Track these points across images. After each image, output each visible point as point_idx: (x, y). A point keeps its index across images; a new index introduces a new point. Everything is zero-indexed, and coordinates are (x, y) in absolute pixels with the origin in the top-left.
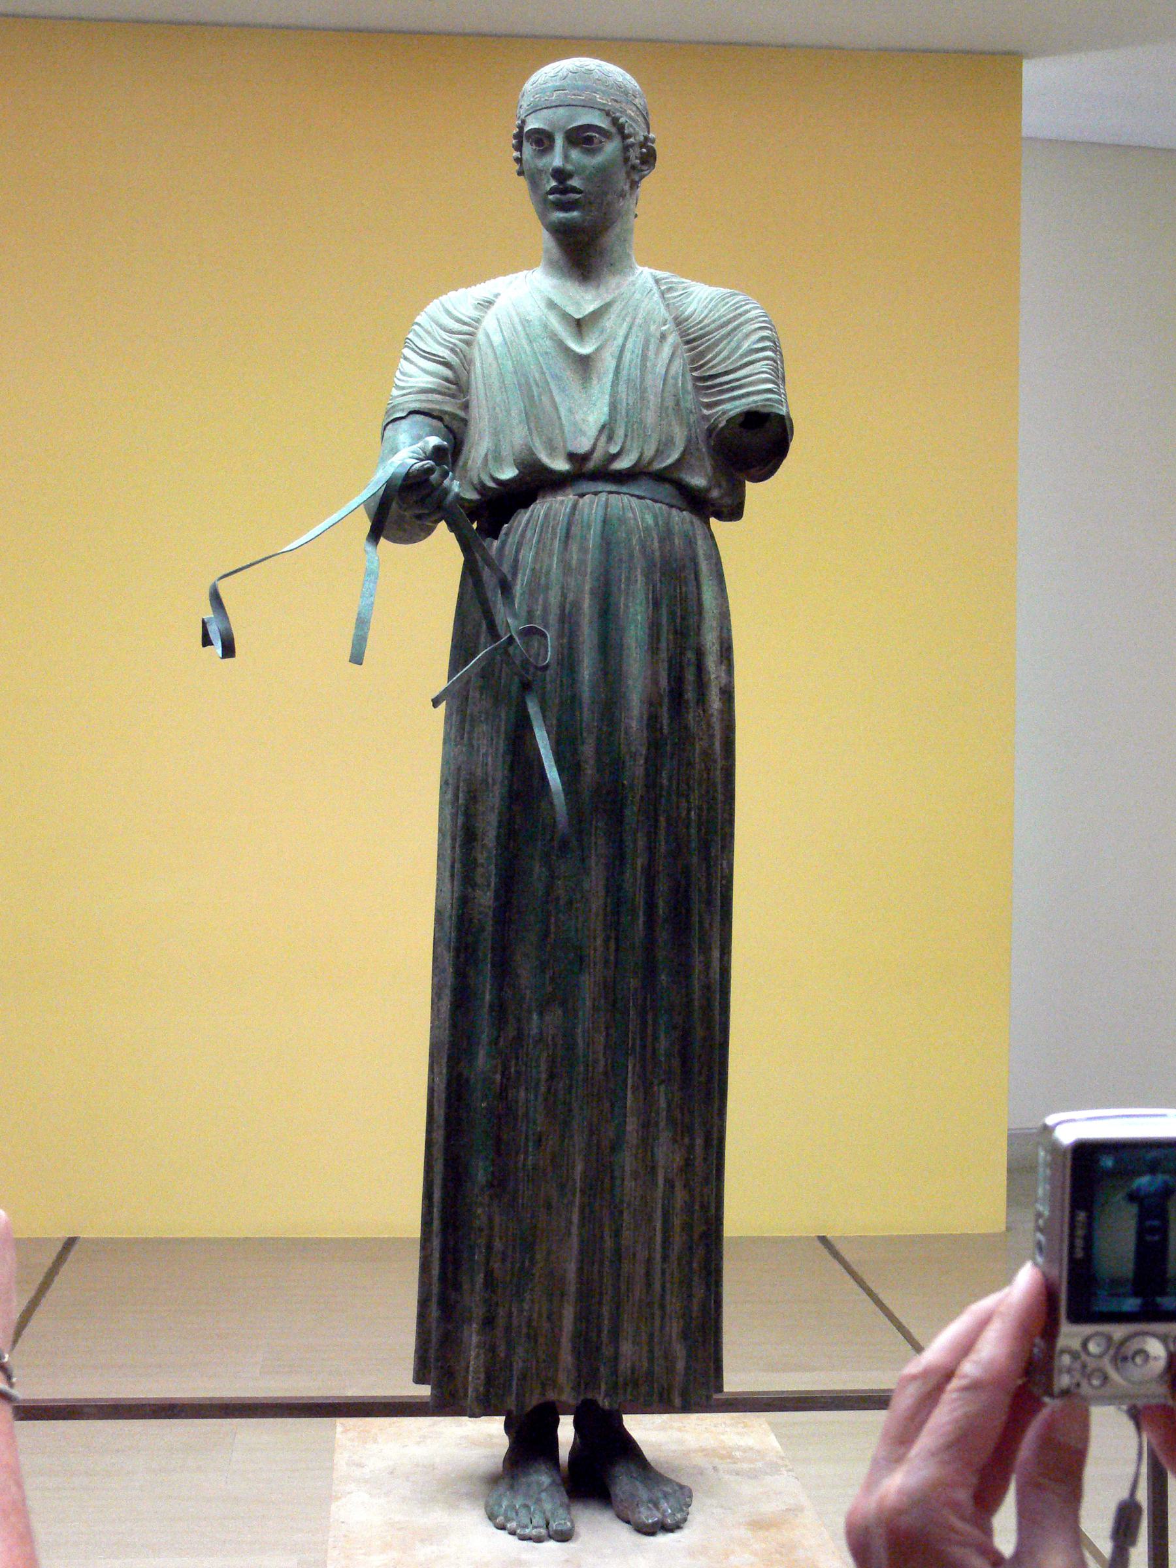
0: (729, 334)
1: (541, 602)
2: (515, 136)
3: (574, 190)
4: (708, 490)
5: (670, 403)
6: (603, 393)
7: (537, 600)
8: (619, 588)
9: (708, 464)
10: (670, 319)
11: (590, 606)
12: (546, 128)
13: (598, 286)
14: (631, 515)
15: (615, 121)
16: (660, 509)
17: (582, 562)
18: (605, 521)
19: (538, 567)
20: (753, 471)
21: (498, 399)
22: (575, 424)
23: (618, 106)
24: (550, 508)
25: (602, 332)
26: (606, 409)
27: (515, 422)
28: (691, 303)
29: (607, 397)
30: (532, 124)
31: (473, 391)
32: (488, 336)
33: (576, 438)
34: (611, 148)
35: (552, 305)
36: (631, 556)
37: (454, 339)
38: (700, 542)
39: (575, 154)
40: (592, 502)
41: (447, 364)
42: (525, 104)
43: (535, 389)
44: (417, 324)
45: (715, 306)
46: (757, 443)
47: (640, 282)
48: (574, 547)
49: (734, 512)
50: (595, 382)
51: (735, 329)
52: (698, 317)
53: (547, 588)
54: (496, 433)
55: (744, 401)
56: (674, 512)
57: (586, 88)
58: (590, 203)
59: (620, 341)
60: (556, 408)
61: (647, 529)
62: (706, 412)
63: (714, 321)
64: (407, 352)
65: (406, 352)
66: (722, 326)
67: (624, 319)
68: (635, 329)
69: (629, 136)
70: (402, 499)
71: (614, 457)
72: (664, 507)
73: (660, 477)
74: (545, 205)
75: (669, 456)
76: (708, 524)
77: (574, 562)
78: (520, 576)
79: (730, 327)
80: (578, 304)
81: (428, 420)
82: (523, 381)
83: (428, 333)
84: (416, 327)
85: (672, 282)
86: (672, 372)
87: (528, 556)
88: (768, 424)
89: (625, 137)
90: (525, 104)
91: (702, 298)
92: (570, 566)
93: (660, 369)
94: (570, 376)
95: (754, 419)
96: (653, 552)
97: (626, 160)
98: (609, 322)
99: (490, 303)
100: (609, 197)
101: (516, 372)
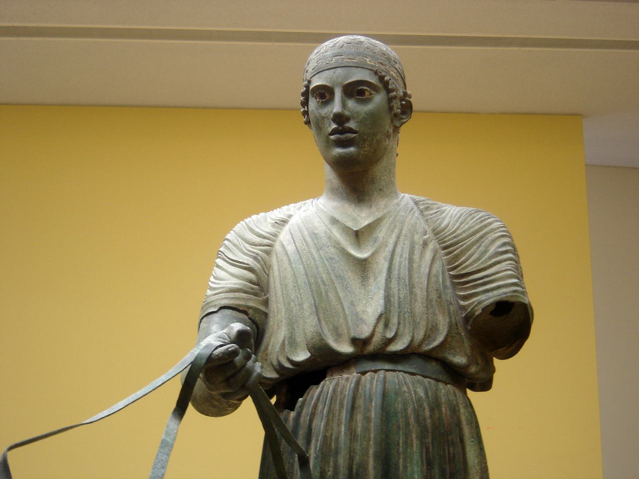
0: (477, 241)
1: (331, 464)
2: (303, 94)
3: (351, 131)
4: (467, 367)
5: (434, 296)
6: (379, 288)
7: (329, 463)
8: (398, 453)
9: (467, 344)
10: (429, 230)
11: (375, 468)
12: (328, 84)
13: (371, 206)
14: (405, 388)
15: (381, 78)
16: (429, 383)
17: (366, 429)
18: (385, 394)
19: (327, 434)
20: (501, 350)
21: (293, 297)
22: (357, 315)
23: (383, 67)
24: (337, 385)
25: (375, 241)
26: (382, 302)
27: (307, 314)
28: (445, 218)
29: (382, 292)
30: (316, 82)
31: (272, 290)
32: (283, 246)
33: (358, 326)
34: (379, 99)
35: (334, 221)
36: (407, 424)
37: (255, 250)
38: (462, 410)
39: (351, 103)
40: (372, 379)
41: (251, 270)
42: (310, 68)
43: (322, 286)
44: (227, 239)
45: (465, 219)
46: (504, 327)
47: (403, 203)
48: (359, 417)
49: (485, 385)
50: (371, 280)
51: (481, 237)
53: (337, 452)
54: (291, 324)
55: (495, 292)
56: (441, 385)
57: (359, 54)
58: (364, 141)
59: (390, 247)
60: (341, 303)
61: (419, 400)
62: (462, 303)
63: (464, 232)
64: (219, 261)
65: (219, 261)
67: (393, 231)
68: (402, 238)
69: (392, 90)
70: (208, 380)
71: (390, 341)
72: (433, 382)
73: (427, 356)
74: (329, 144)
75: (434, 340)
76: (465, 393)
77: (359, 430)
78: (313, 442)
79: (478, 235)
80: (354, 220)
81: (235, 313)
82: (312, 280)
83: (235, 245)
84: (226, 242)
85: (428, 204)
86: (434, 271)
87: (319, 424)
88: (512, 313)
89: (389, 91)
90: (310, 68)
91: (452, 214)
92: (355, 433)
93: (425, 270)
94: (351, 277)
95: (502, 308)
96: (425, 419)
97: (391, 109)
98: (381, 233)
99: (284, 222)
100: (378, 137)
101: (306, 274)
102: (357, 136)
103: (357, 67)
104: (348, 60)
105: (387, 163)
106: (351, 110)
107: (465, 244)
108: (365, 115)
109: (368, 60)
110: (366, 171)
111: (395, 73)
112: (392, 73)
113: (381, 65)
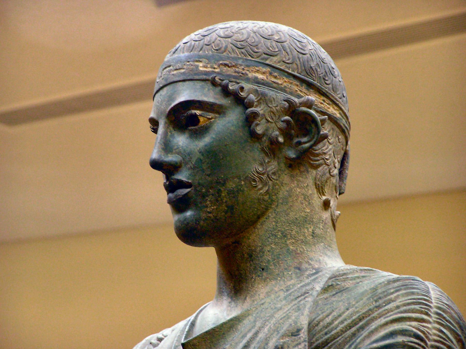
0: (354, 335)
13: (245, 299)
23: (230, 71)
39: (181, 140)
52: (328, 320)
58: (204, 196)
63: (342, 322)
66: (354, 323)
69: (250, 105)
97: (254, 136)
100: (231, 185)
102: (193, 191)
103: (184, 81)
104: (175, 72)
105: (277, 222)
106: (182, 152)
107: (338, 341)
108: (198, 155)
109: (201, 64)
110: (237, 243)
111: (264, 73)
112: (250, 75)
113: (225, 69)
